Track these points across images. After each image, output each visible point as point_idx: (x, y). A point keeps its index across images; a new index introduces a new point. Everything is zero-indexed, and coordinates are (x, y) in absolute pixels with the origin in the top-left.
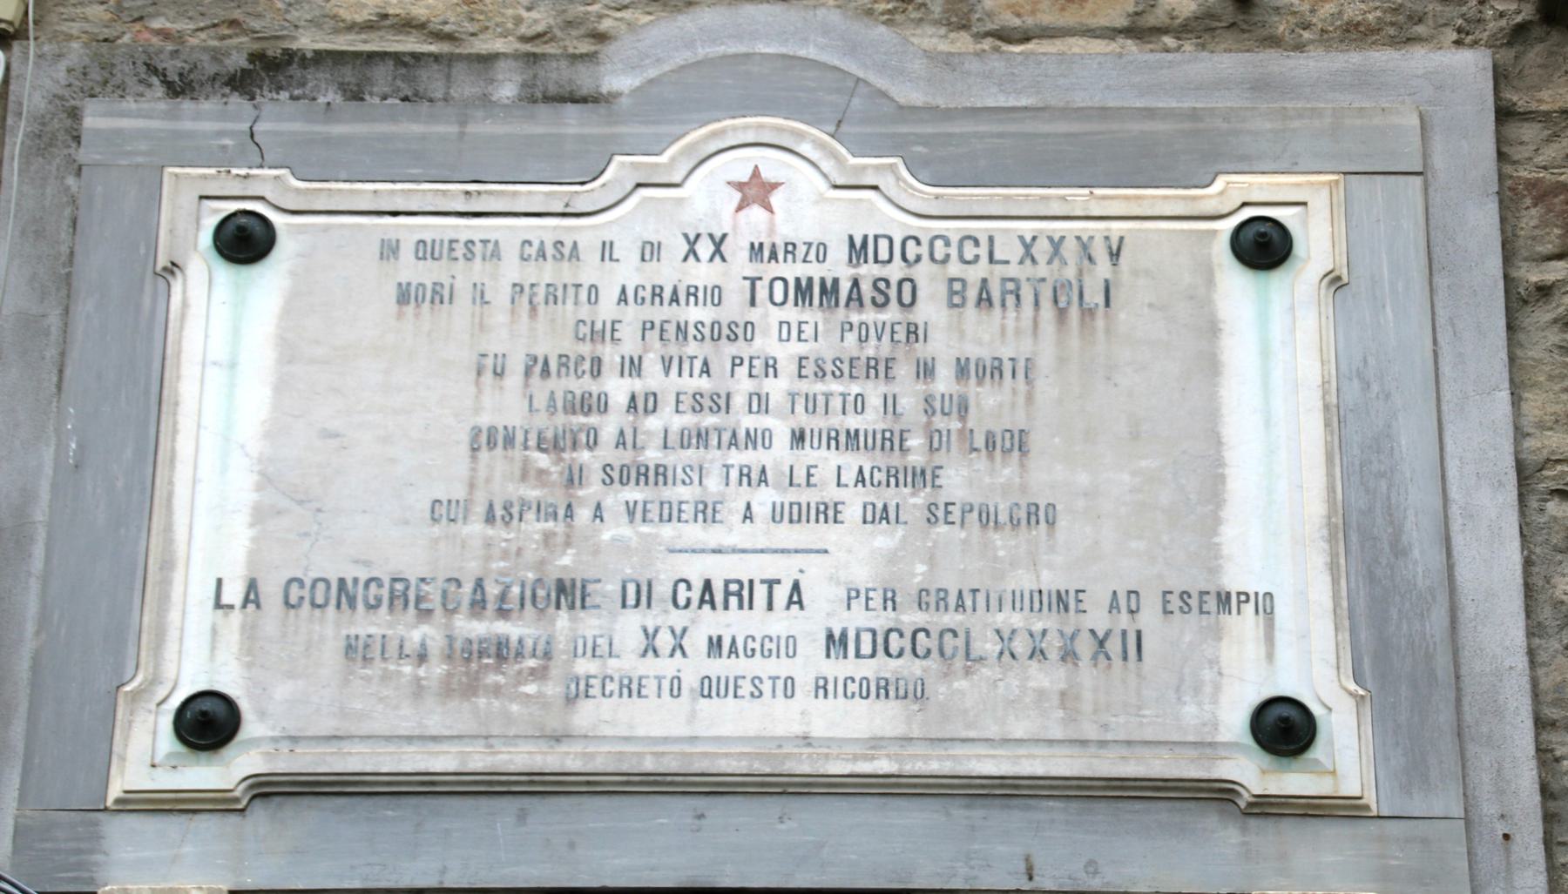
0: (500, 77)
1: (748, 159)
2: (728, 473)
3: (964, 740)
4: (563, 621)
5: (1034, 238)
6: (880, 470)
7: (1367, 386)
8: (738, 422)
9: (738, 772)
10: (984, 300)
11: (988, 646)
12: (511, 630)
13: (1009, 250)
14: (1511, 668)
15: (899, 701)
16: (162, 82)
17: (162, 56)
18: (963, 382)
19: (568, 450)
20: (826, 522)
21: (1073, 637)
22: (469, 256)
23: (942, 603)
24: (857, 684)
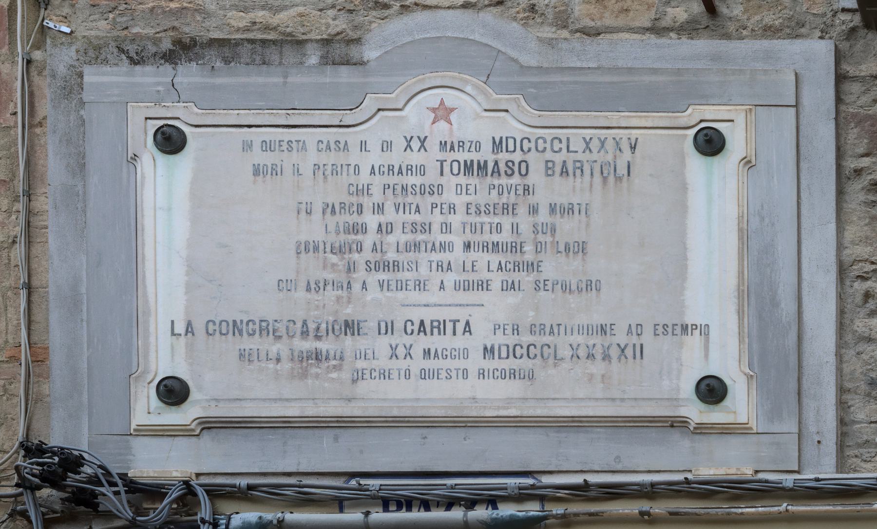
0: (309, 52)
1: (438, 95)
2: (431, 265)
3: (554, 399)
4: (348, 341)
5: (591, 139)
6: (510, 263)
7: (762, 219)
8: (436, 238)
9: (441, 416)
10: (564, 172)
11: (566, 353)
12: (323, 346)
13: (577, 145)
14: (827, 362)
15: (521, 380)
16: (127, 57)
17: (126, 43)
18: (553, 216)
19: (347, 254)
20: (482, 290)
21: (608, 348)
22: (290, 149)
23: (542, 331)
24: (500, 372)
